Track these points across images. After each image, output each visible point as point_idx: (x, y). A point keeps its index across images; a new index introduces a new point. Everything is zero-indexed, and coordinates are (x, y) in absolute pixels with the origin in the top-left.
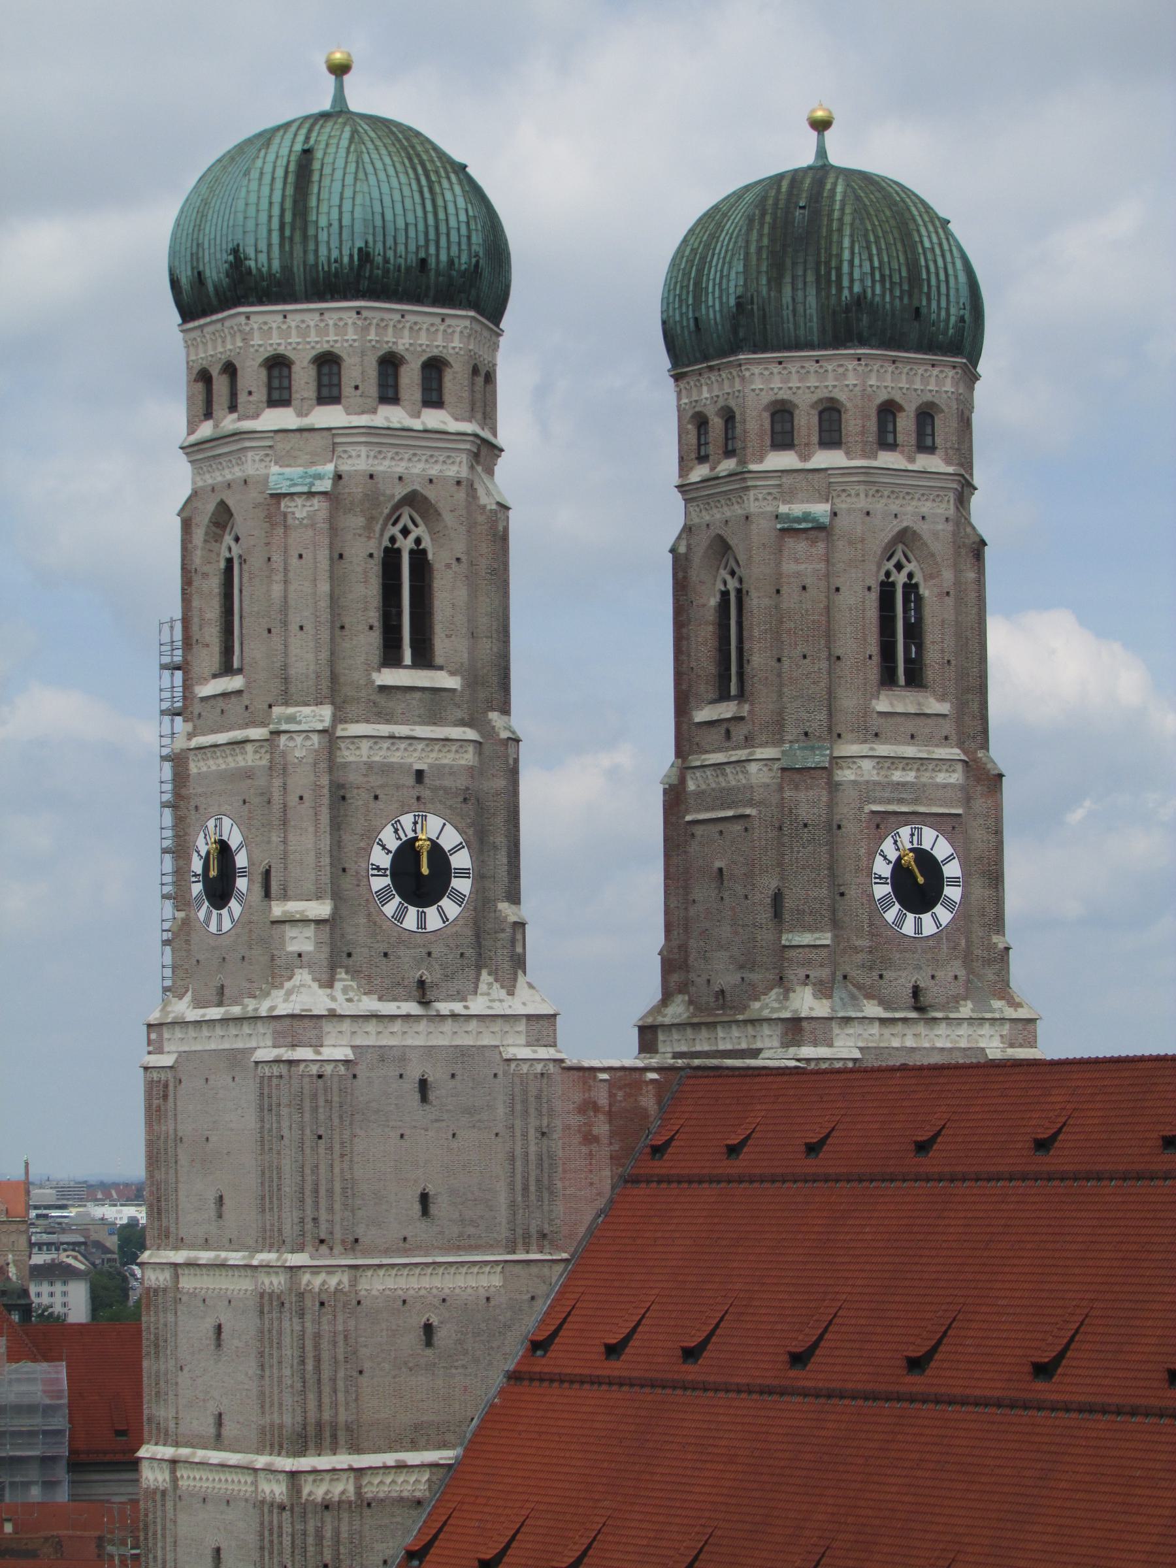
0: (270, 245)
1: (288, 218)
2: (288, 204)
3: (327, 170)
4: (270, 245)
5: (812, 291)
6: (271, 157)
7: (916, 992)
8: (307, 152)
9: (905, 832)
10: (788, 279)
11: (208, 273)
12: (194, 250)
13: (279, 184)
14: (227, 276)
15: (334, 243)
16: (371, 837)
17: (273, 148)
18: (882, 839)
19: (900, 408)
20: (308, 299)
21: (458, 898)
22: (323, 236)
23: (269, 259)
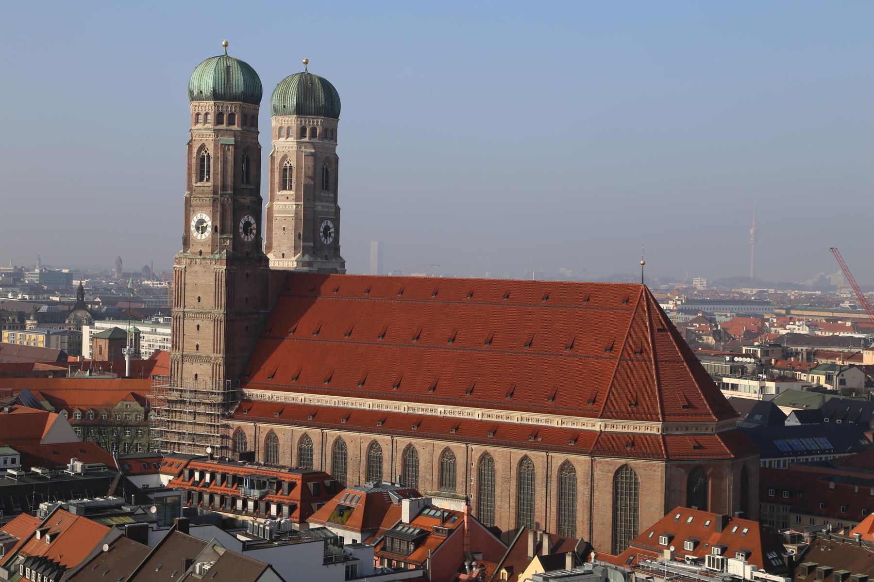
0: (221, 88)
1: (226, 82)
2: (226, 79)
3: (234, 72)
4: (221, 88)
5: (313, 103)
6: (219, 67)
7: (326, 256)
8: (228, 68)
9: (326, 221)
10: (308, 100)
11: (203, 92)
12: (199, 85)
13: (223, 74)
14: (210, 93)
15: (237, 89)
16: (240, 221)
17: (219, 65)
18: (322, 223)
19: (328, 130)
20: (229, 100)
21: (253, 234)
22: (234, 87)
23: (221, 91)
